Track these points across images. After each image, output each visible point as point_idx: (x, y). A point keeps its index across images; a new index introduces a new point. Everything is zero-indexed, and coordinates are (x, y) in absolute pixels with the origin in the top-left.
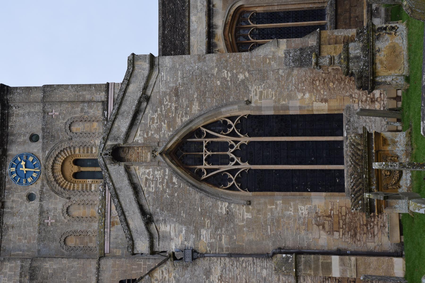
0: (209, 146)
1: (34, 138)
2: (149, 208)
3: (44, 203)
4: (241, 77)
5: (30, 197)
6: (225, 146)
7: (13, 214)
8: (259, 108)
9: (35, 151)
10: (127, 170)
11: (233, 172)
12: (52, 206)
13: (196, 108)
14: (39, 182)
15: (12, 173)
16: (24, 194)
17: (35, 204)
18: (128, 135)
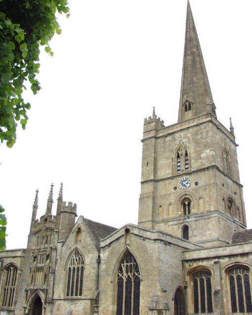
1: (196, 184)
9: (192, 185)
10: (123, 235)
17: (173, 191)
18: (133, 234)
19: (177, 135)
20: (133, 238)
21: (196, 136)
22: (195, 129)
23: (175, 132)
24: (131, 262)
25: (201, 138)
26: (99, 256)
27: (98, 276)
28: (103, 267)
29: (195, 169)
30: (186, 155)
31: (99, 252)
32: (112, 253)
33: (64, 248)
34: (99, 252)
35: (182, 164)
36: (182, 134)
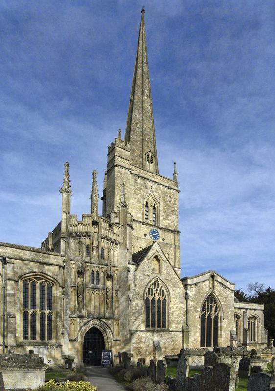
0: (211, 306)
1: (164, 240)
2: (199, 285)
3: (144, 239)
4: (229, 317)
5: (145, 235)
6: (211, 311)
7: (140, 227)
8: (221, 322)
11: (205, 313)
12: (143, 242)
13: (222, 303)
14: (151, 239)
15: (153, 230)
16: (147, 233)
17: (143, 236)
18: (217, 281)
19: (149, 184)
20: (216, 284)
21: (166, 197)
22: (166, 189)
23: (148, 179)
24: (212, 304)
25: (170, 202)
26: (186, 293)
27: (187, 311)
28: (191, 303)
29: (163, 227)
30: (154, 208)
31: (186, 289)
32: (198, 292)
33: (137, 272)
34: (186, 289)
35: (151, 215)
36: (155, 186)
